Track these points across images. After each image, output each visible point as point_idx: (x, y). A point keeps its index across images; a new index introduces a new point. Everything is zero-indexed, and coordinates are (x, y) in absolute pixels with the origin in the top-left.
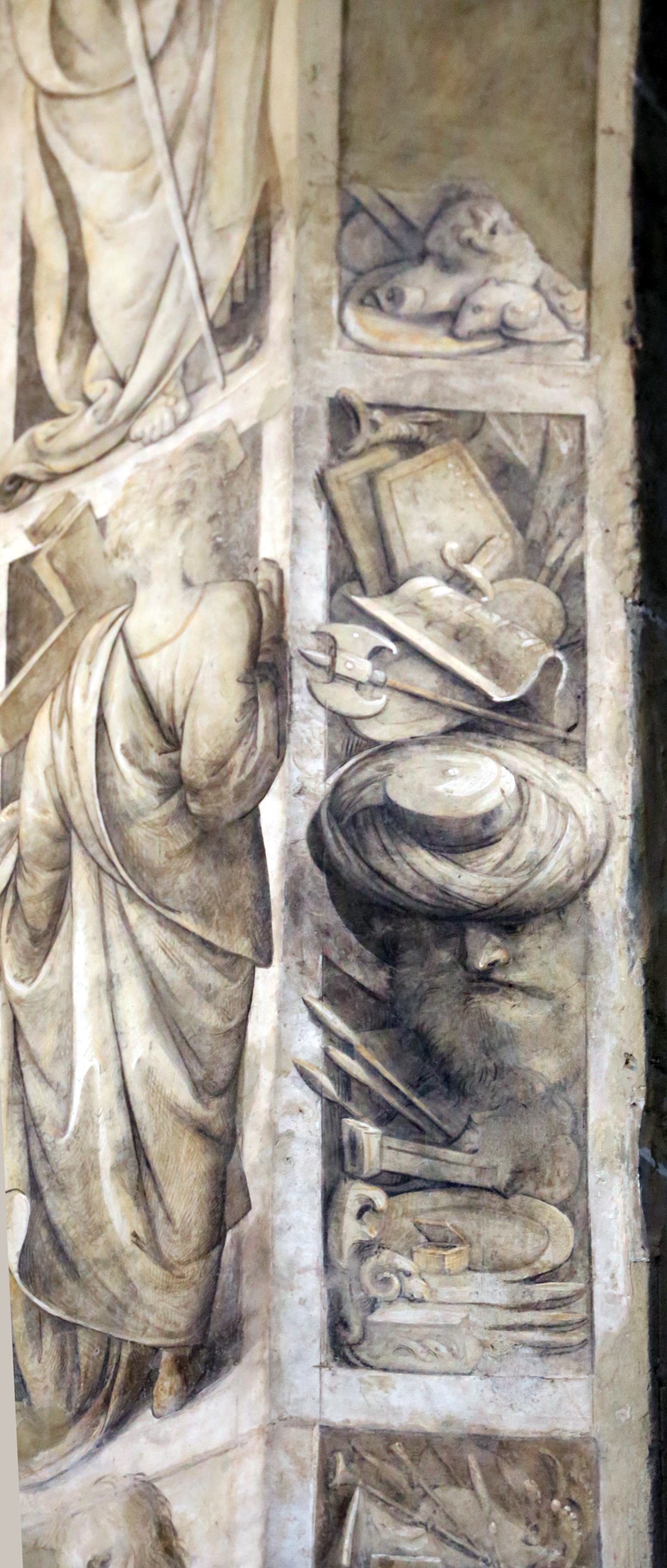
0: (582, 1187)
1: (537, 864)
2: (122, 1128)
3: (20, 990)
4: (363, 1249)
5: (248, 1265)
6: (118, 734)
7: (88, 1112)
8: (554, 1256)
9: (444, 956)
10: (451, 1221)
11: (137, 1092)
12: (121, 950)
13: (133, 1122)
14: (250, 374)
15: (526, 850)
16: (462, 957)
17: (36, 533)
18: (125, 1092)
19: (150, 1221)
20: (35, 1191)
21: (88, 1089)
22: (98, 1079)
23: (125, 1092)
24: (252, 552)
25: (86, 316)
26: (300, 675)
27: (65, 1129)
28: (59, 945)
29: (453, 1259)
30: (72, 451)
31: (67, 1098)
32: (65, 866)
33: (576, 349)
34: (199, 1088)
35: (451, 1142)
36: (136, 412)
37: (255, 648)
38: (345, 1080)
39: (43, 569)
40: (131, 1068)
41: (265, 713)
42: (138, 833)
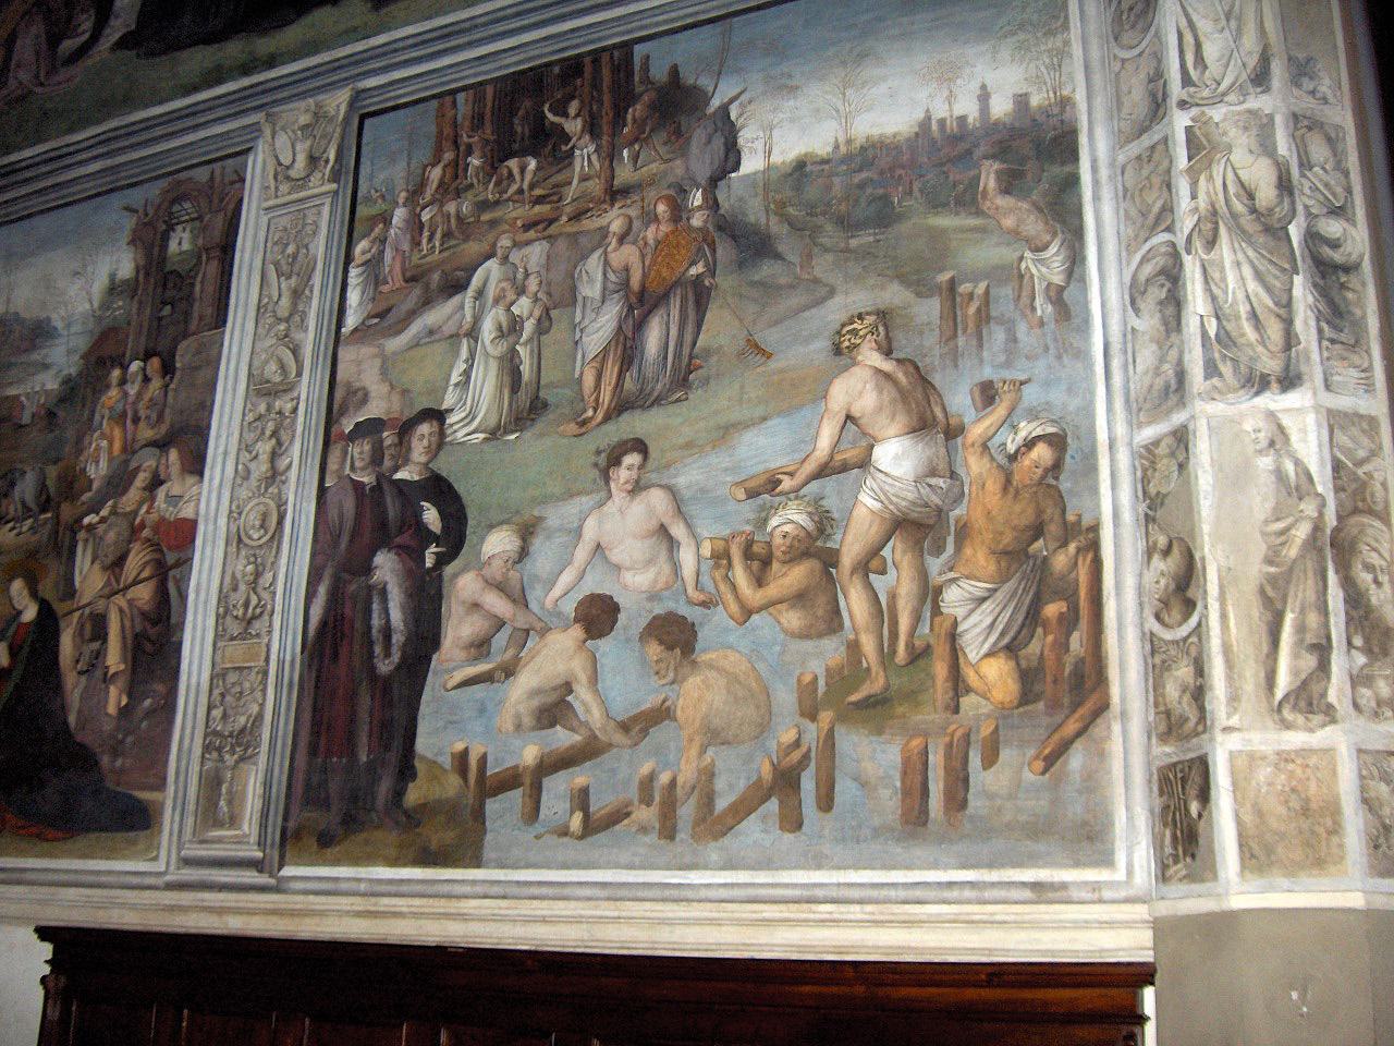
0: (1369, 348)
1: (1350, 254)
2: (1248, 308)
3: (1205, 257)
4: (1328, 359)
5: (1302, 360)
6: (1232, 189)
7: (1234, 298)
8: (1366, 365)
9: (1334, 278)
10: (1346, 354)
11: (1253, 299)
12: (1241, 256)
13: (1253, 308)
14: (1264, 97)
15: (1349, 249)
16: (1338, 279)
17: (1193, 120)
18: (1248, 297)
19: (1262, 337)
20: (1218, 318)
21: (1234, 293)
22: (1238, 291)
23: (1248, 297)
24: (1275, 149)
25: (1203, 59)
26: (1297, 192)
27: (1226, 301)
28: (1217, 247)
29: (1346, 363)
30: (1202, 99)
31: (1226, 293)
32: (1217, 223)
33: (1339, 108)
34: (1276, 304)
35: (1341, 331)
36: (1224, 94)
37: (1280, 178)
38: (1319, 311)
39: (1198, 132)
40: (1250, 291)
41: (1287, 200)
42: (1243, 221)
